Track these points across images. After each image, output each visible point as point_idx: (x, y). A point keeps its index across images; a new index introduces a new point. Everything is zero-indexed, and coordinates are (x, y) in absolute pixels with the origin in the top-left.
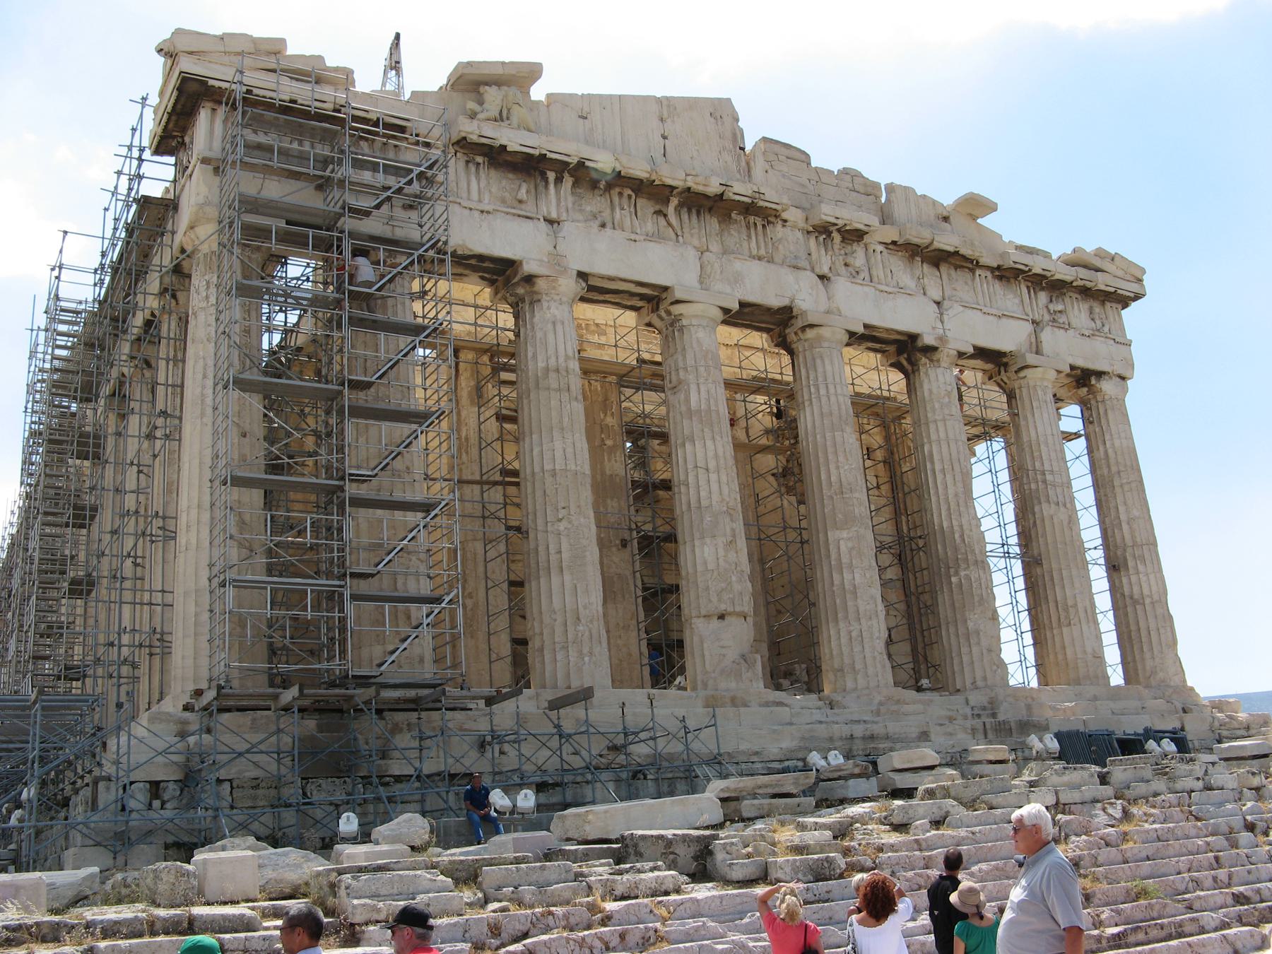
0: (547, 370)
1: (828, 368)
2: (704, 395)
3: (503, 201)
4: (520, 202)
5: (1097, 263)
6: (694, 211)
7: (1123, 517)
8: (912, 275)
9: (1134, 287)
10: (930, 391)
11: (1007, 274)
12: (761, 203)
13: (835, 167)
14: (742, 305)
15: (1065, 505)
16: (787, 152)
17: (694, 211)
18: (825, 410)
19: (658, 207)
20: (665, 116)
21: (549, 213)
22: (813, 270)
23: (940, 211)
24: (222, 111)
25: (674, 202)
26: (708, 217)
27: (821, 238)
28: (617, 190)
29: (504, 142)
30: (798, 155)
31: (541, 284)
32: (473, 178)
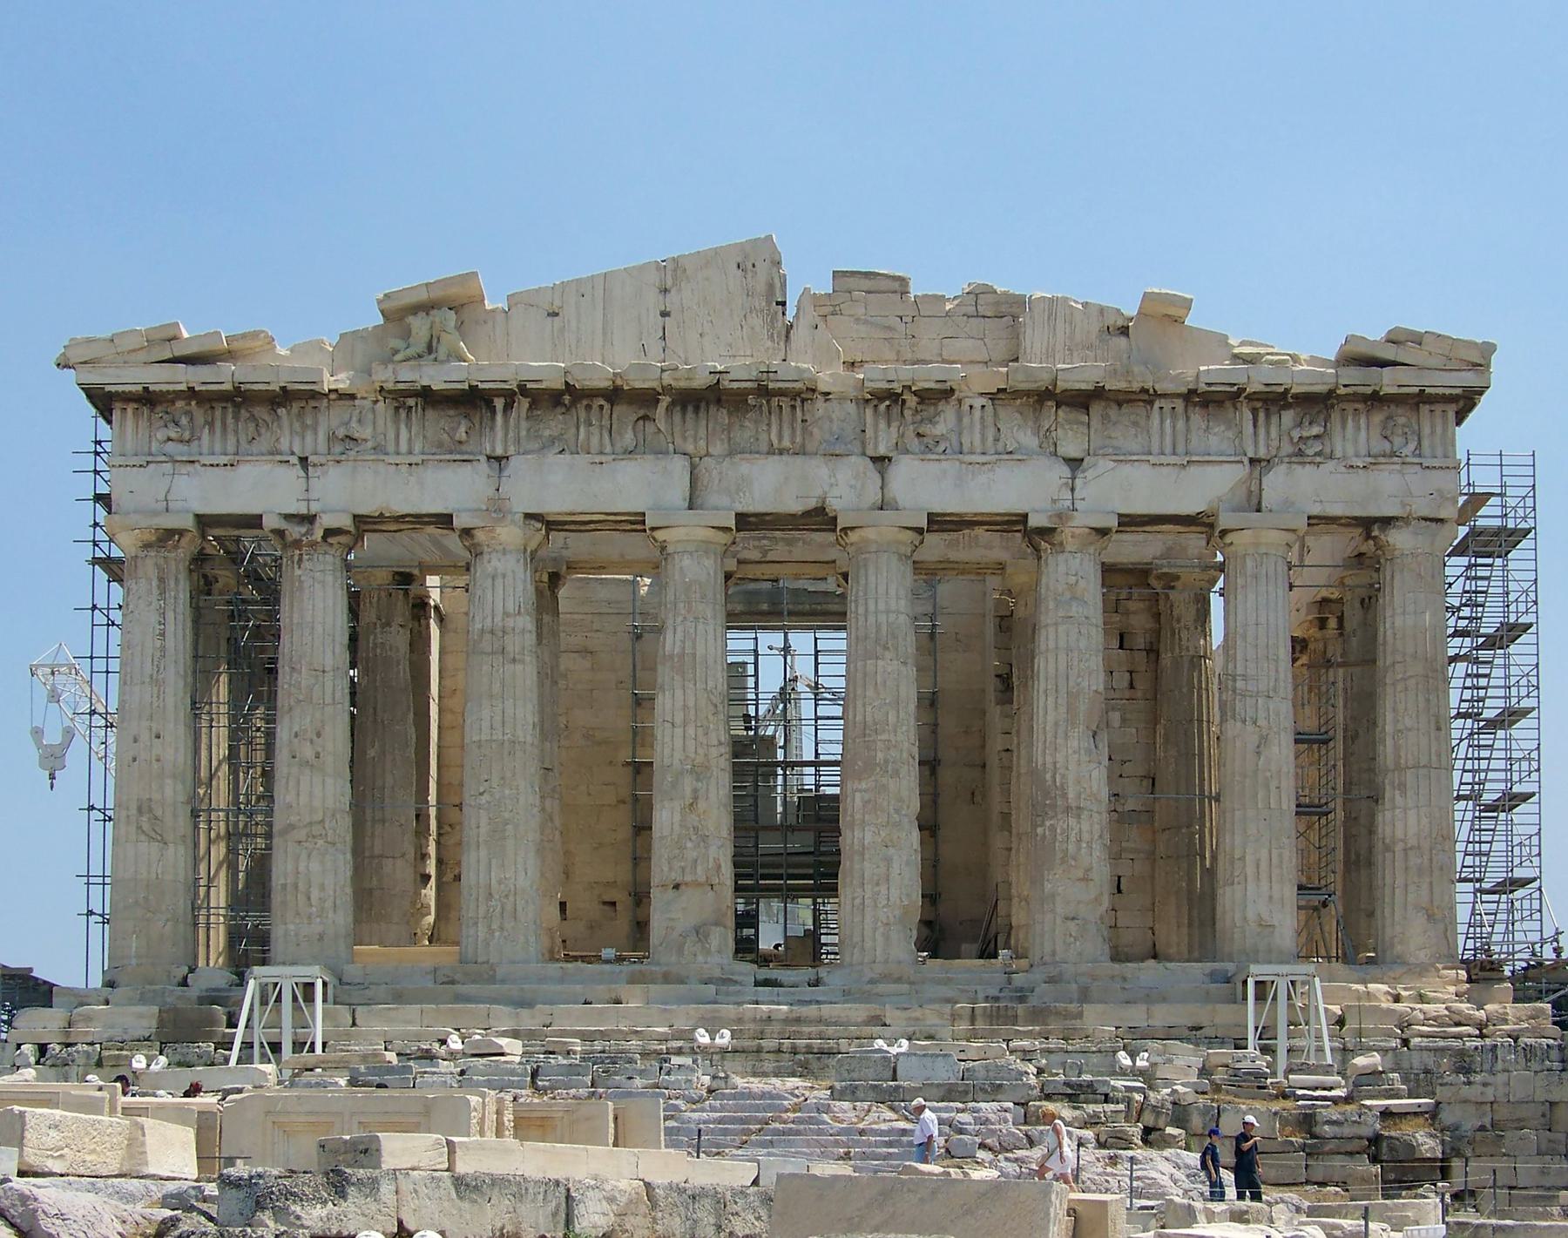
1: (872, 579)
2: (679, 635)
5: (1389, 353)
6: (690, 408)
8: (1037, 432)
10: (1048, 588)
11: (1207, 400)
15: (1255, 723)
16: (867, 284)
17: (690, 408)
19: (641, 413)
20: (669, 283)
21: (494, 450)
22: (864, 454)
25: (665, 400)
26: (713, 409)
27: (882, 407)
28: (585, 402)
30: (884, 285)
32: (403, 426)
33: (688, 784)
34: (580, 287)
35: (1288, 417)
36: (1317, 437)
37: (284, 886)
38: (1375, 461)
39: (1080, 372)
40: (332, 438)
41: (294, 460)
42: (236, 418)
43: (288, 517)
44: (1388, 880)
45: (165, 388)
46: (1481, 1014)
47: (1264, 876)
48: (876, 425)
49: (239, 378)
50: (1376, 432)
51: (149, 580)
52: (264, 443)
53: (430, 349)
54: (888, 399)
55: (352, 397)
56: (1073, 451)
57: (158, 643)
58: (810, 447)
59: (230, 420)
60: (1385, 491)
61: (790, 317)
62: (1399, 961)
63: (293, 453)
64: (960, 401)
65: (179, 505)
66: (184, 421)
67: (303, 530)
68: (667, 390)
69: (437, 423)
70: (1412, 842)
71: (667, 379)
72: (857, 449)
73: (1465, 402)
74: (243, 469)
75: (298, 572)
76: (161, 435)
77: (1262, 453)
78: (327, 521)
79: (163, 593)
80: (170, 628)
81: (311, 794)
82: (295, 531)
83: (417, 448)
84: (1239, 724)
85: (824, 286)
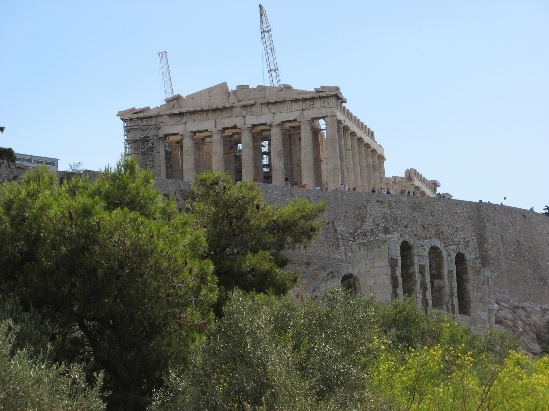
35: (308, 102)
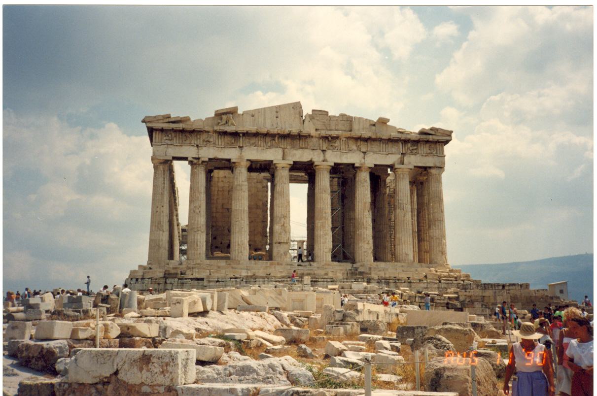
0: (237, 185)
1: (322, 176)
3: (228, 144)
4: (233, 143)
7: (431, 212)
8: (356, 146)
9: (448, 138)
12: (301, 134)
13: (337, 115)
14: (294, 162)
15: (403, 209)
16: (320, 113)
18: (319, 188)
23: (372, 123)
24: (157, 132)
29: (226, 130)
30: (324, 113)
31: (237, 164)
33: (283, 220)
34: (259, 111)
35: (409, 145)
36: (415, 149)
37: (191, 242)
38: (427, 155)
39: (366, 134)
40: (204, 141)
41: (195, 145)
42: (182, 135)
43: (193, 158)
44: (433, 245)
45: (167, 128)
46: (455, 276)
47: (406, 243)
48: (323, 143)
49: (184, 127)
50: (428, 149)
51: (161, 171)
52: (188, 142)
53: (227, 123)
54: (326, 138)
55: (208, 132)
56: (364, 150)
57: (163, 185)
58: (309, 148)
59: (180, 136)
60: (429, 161)
61: (304, 118)
62: (436, 263)
63: (195, 144)
64: (340, 139)
65: (169, 154)
66: (170, 136)
67: (197, 161)
68: (278, 134)
69: (228, 139)
70: (438, 237)
71: (279, 132)
72: (318, 148)
73: (447, 142)
74: (183, 147)
75: (195, 170)
76: (165, 138)
77: (404, 152)
78: (203, 159)
79: (164, 174)
80: (166, 182)
81: (198, 221)
82: (195, 161)
83: (223, 144)
84: (400, 210)
85: (310, 113)
